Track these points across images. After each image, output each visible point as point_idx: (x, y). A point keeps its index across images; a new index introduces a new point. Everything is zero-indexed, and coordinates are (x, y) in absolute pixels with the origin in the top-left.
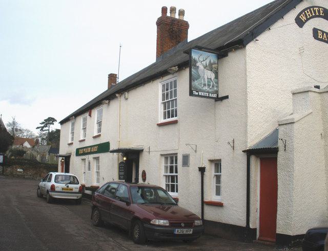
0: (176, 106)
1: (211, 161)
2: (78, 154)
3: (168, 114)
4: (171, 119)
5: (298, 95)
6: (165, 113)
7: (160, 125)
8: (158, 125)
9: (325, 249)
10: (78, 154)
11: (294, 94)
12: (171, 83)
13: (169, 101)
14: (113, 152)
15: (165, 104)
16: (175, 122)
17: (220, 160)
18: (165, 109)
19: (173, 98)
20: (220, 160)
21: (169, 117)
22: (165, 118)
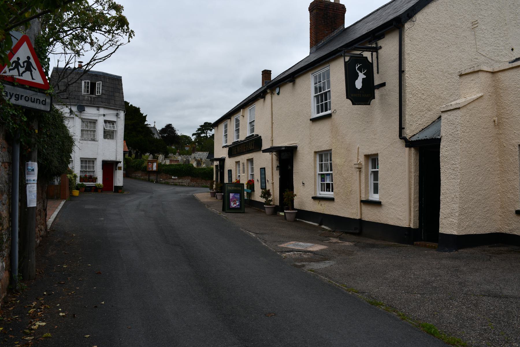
0: (330, 99)
1: (367, 156)
2: (231, 154)
3: (320, 108)
4: (324, 113)
5: (467, 76)
6: (318, 107)
7: (314, 120)
8: (311, 120)
9: (518, 209)
10: (231, 154)
11: (461, 75)
12: (324, 73)
13: (322, 94)
14: (265, 151)
15: (317, 97)
16: (329, 116)
17: (377, 155)
18: (318, 102)
19: (327, 90)
20: (377, 155)
21: (322, 111)
22: (318, 113)
